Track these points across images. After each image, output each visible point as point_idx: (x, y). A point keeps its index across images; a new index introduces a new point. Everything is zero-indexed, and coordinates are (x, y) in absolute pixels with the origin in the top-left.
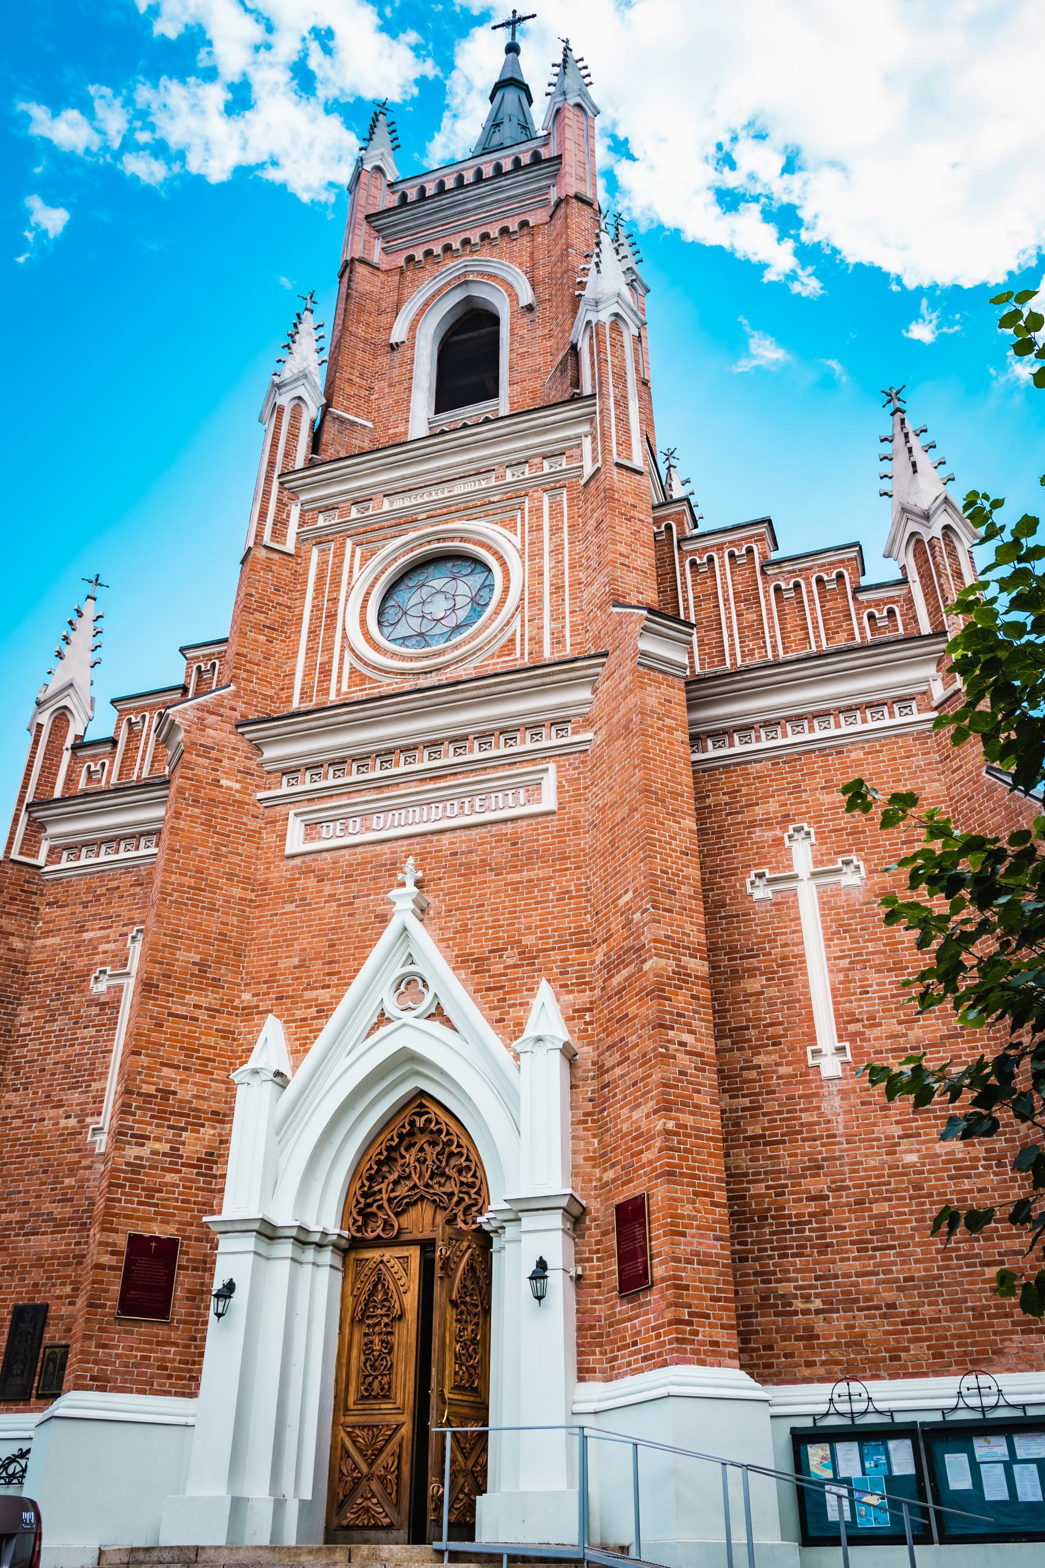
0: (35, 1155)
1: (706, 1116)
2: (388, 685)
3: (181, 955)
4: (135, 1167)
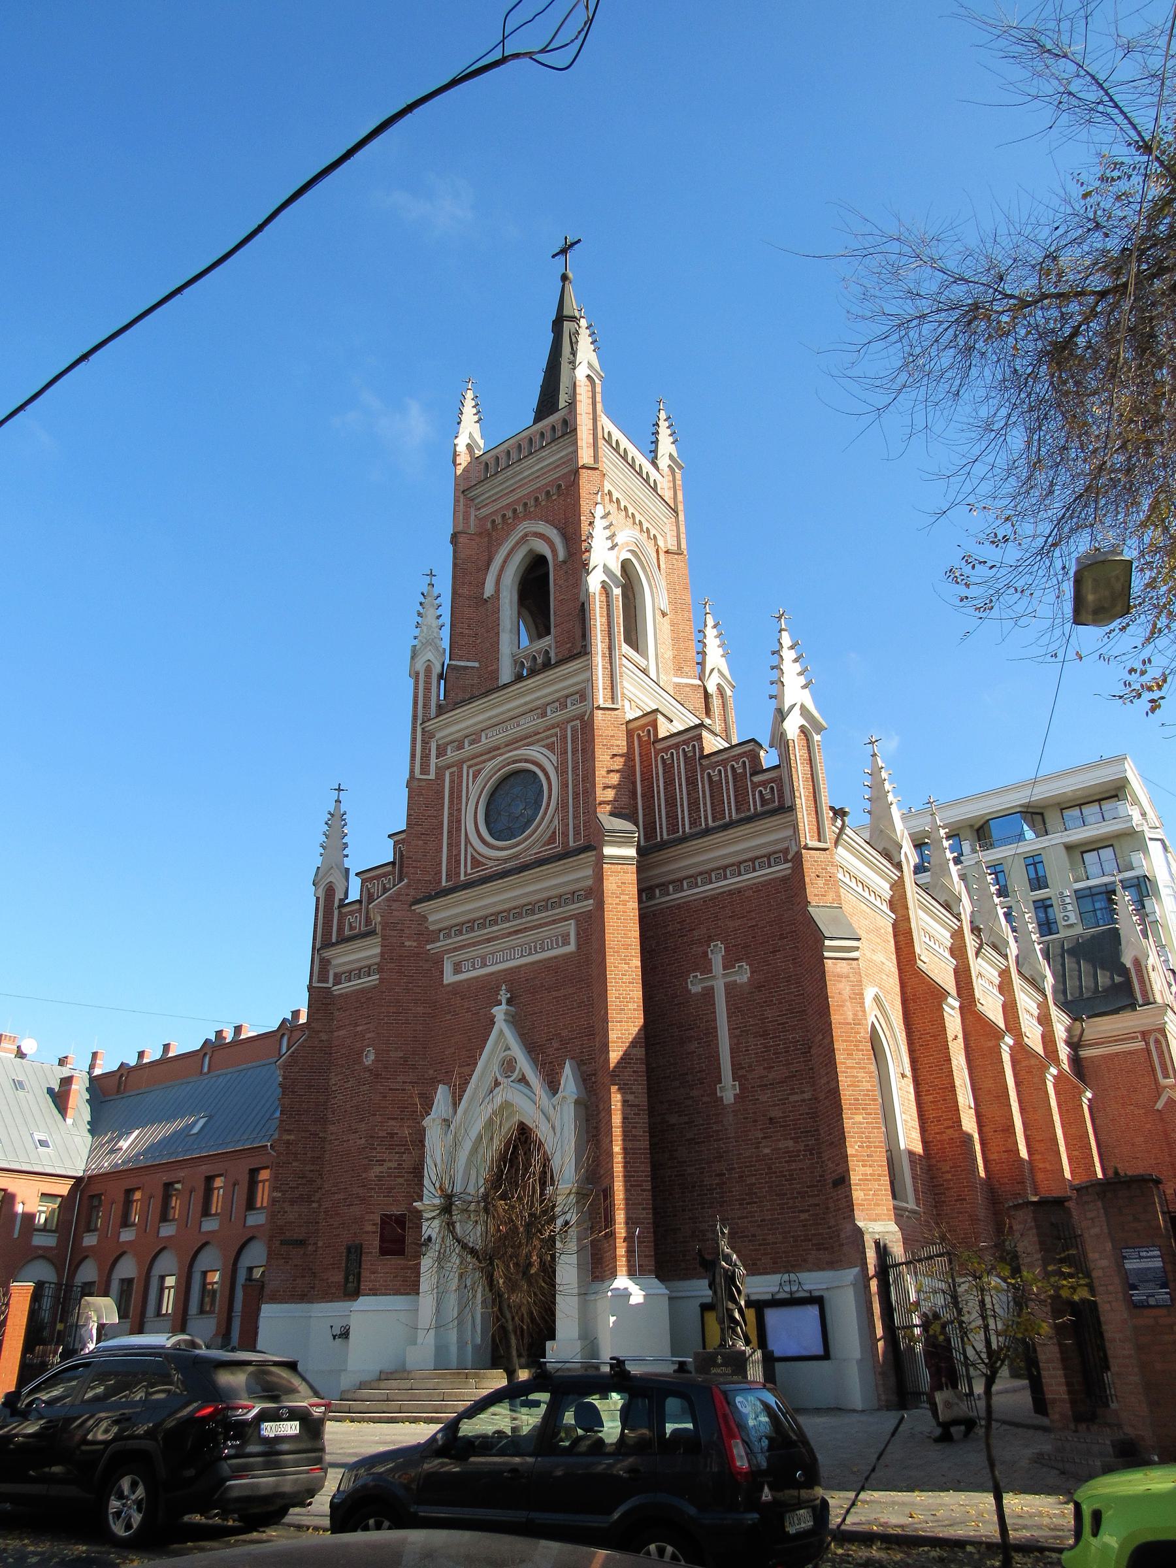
1: (640, 1141)
2: (491, 867)
3: (392, 1054)
4: (380, 1178)
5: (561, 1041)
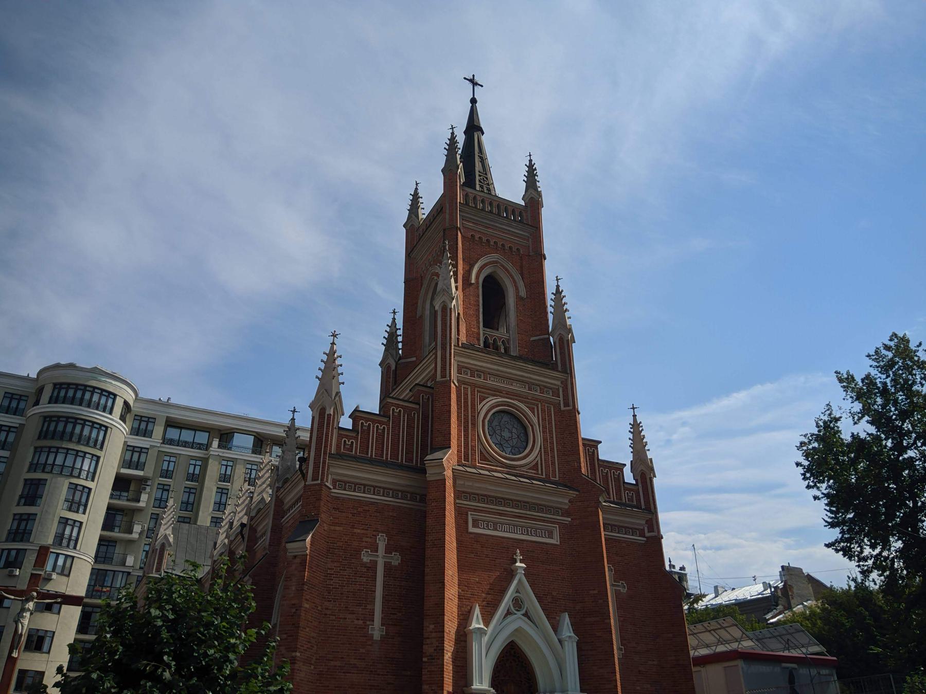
0: (344, 635)
5: (552, 598)
